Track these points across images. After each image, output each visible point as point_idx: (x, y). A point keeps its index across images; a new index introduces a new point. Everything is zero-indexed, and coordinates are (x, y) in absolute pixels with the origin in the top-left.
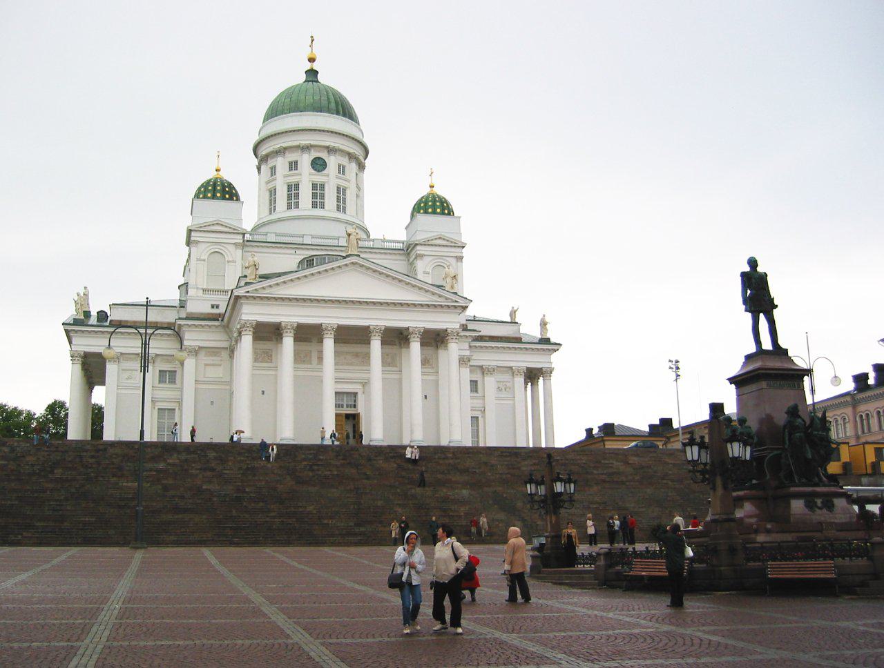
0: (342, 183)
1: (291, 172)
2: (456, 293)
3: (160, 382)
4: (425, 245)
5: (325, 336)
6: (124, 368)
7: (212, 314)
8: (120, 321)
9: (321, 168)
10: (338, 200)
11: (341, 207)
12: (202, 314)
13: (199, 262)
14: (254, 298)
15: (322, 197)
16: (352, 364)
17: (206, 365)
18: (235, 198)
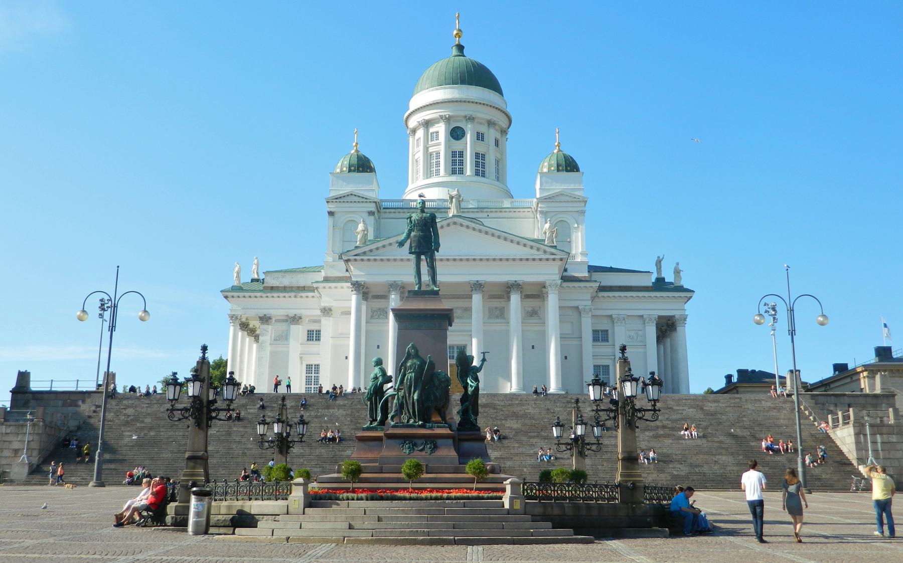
0: (481, 150)
2: (555, 247)
3: (308, 340)
4: (545, 202)
8: (272, 287)
12: (336, 277)
15: (462, 163)
18: (368, 171)
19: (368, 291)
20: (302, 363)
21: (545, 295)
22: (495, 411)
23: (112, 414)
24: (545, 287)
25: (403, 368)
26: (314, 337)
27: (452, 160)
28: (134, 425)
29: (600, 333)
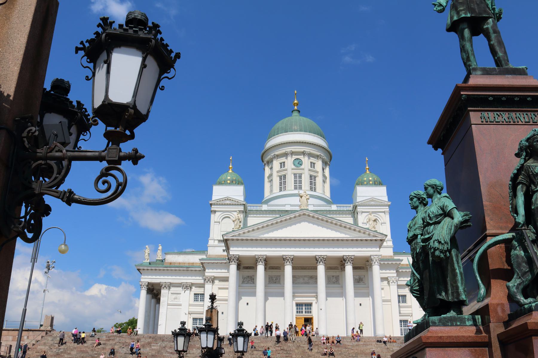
1: (281, 169)
3: (195, 301)
5: (285, 264)
6: (172, 292)
7: (223, 255)
8: (171, 263)
9: (300, 163)
10: (311, 183)
11: (313, 186)
12: (216, 256)
13: (215, 223)
14: (238, 240)
15: (300, 182)
16: (308, 283)
17: (220, 288)
18: (239, 183)
19: (240, 263)
20: (190, 317)
21: (368, 267)
22: (347, 350)
23: (47, 347)
24: (368, 261)
25: (520, 178)
26: (199, 299)
27: (294, 180)
28: (62, 356)
29: (401, 298)
